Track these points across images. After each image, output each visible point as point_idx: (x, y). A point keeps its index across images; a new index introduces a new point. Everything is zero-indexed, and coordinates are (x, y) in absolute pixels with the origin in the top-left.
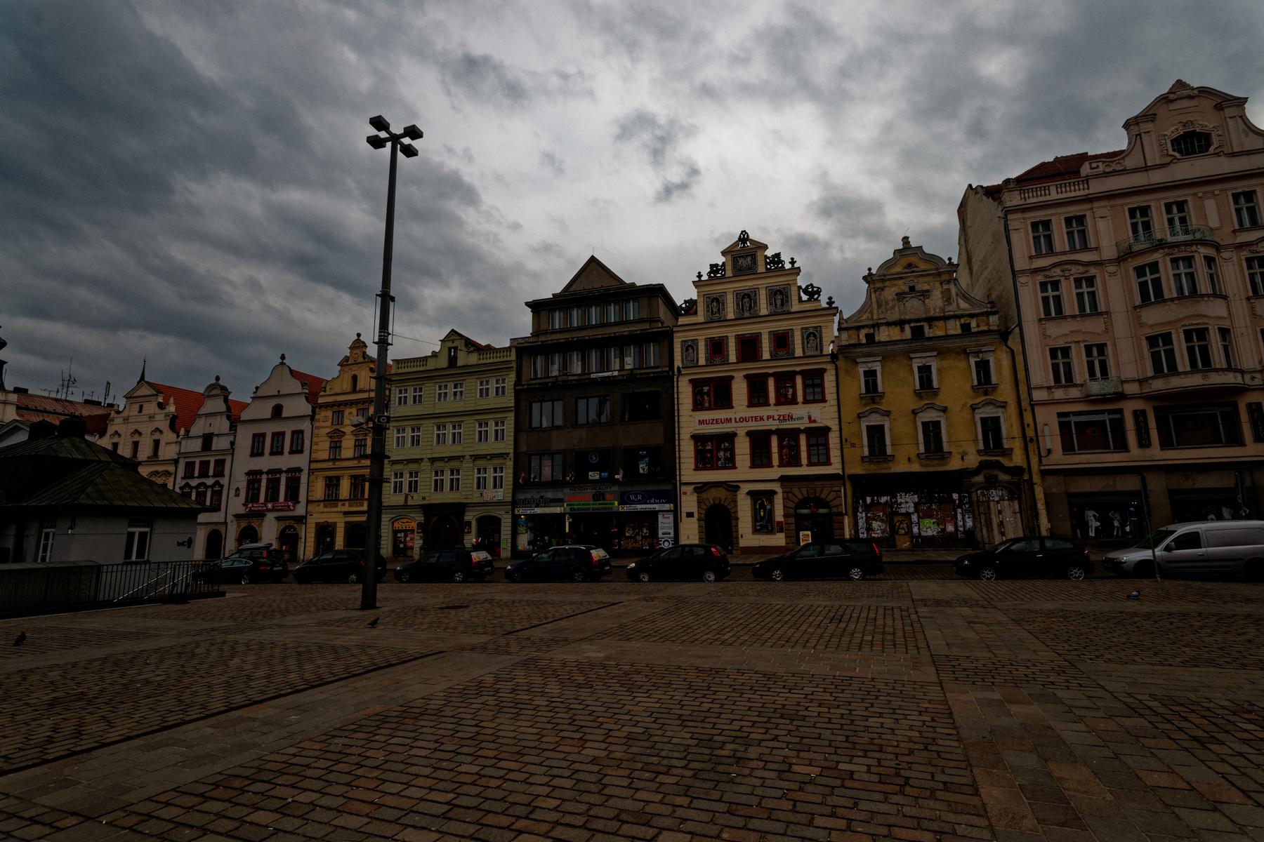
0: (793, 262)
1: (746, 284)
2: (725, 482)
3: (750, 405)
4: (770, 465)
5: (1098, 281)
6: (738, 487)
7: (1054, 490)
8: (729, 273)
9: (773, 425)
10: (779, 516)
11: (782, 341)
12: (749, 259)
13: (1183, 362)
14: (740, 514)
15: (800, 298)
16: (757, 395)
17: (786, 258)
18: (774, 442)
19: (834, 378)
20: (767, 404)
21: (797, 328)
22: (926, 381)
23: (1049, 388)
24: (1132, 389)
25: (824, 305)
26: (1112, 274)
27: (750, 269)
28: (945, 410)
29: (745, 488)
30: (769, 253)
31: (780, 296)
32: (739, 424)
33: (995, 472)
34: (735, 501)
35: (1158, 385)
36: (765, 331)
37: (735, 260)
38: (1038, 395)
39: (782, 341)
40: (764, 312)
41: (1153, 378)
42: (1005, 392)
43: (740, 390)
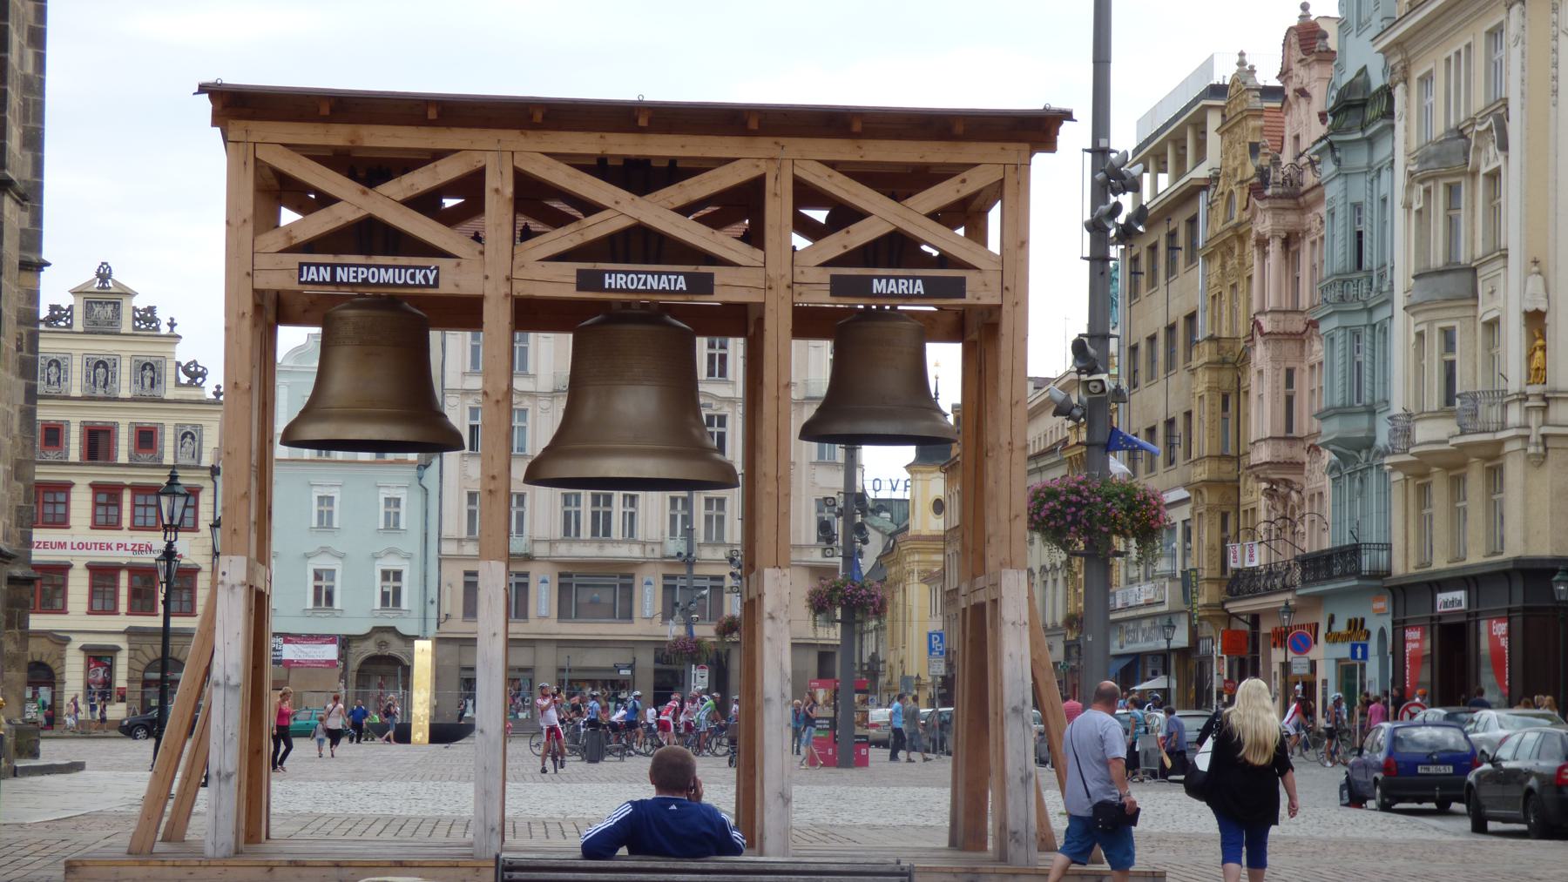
0: (172, 325)
1: (102, 347)
2: (50, 632)
3: (95, 526)
4: (114, 611)
5: (529, 415)
6: (68, 640)
7: (447, 662)
8: (78, 326)
9: (123, 557)
10: (121, 680)
11: (146, 438)
12: (110, 308)
13: (586, 532)
14: (67, 676)
15: (178, 379)
16: (105, 518)
17: (163, 316)
18: (124, 578)
19: (211, 500)
20: (117, 526)
21: (169, 424)
22: (325, 521)
23: (460, 540)
24: (541, 550)
25: (210, 395)
26: (545, 410)
27: (110, 323)
28: (341, 557)
29: (78, 642)
30: (140, 302)
31: (149, 370)
32: (77, 552)
33: (387, 637)
34: (62, 658)
35: (565, 551)
36: (124, 423)
37: (89, 306)
38: (449, 548)
39: (146, 438)
40: (125, 393)
41: (561, 541)
42: (413, 544)
43: (81, 504)
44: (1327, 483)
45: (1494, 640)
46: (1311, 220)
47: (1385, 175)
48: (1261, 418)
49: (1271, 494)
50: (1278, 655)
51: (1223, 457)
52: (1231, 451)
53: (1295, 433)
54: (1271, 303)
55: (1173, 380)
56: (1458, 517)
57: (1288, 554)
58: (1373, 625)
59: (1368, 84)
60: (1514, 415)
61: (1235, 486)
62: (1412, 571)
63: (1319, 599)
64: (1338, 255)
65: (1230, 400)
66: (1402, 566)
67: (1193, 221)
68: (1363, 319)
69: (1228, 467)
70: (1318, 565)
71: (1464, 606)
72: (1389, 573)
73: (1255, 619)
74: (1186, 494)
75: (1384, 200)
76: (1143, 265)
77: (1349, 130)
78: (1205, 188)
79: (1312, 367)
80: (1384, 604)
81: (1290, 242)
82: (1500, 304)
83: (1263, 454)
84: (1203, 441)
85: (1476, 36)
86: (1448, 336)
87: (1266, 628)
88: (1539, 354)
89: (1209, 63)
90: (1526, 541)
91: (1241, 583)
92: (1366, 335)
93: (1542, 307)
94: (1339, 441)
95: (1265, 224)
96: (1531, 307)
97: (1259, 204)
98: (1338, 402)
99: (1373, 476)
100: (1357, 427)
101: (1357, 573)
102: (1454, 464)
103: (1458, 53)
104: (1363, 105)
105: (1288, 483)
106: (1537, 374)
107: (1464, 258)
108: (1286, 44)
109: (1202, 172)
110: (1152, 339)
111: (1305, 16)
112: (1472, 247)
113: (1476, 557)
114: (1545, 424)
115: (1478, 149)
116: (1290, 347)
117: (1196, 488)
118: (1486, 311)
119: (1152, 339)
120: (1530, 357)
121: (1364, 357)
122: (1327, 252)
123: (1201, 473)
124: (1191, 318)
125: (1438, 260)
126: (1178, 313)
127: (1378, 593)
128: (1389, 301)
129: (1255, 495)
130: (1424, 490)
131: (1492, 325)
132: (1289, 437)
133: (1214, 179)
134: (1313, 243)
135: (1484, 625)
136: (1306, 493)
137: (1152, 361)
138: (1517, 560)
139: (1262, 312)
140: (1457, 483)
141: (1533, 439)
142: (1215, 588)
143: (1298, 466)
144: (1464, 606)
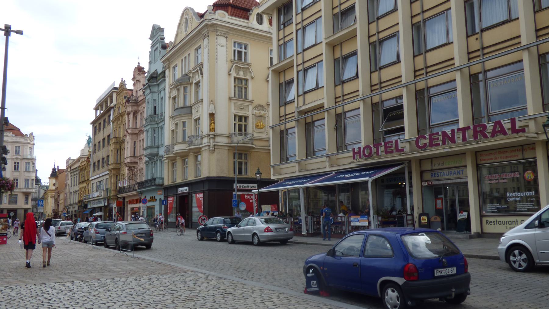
44: (144, 166)
45: (198, 199)
46: (141, 108)
47: (162, 92)
48: (128, 152)
49: (129, 170)
50: (130, 206)
51: (117, 163)
52: (119, 162)
53: (136, 155)
54: (131, 126)
55: (104, 150)
56: (184, 169)
57: (133, 182)
58: (158, 198)
59: (157, 73)
60: (205, 140)
61: (119, 170)
62: (170, 183)
63: (142, 193)
64: (151, 112)
65: (119, 150)
66: (167, 182)
67: (109, 116)
68: (156, 126)
69: (118, 165)
70: (141, 185)
71: (187, 191)
72: (163, 185)
73: (124, 198)
74: (107, 172)
75: (162, 98)
76: (98, 127)
77: (153, 82)
78: (113, 108)
79: (140, 141)
80: (161, 192)
81: (135, 113)
82: (200, 113)
83: (128, 160)
84: (112, 160)
85: (192, 52)
86: (184, 123)
87: (127, 200)
88: (213, 124)
89: (114, 83)
90: (209, 173)
91: (122, 190)
92: (157, 129)
93: (214, 112)
94: (150, 154)
95: (129, 109)
96: (211, 112)
97: (128, 105)
98: (149, 145)
99: (158, 162)
100: (154, 151)
101: (156, 185)
102: (184, 156)
103: (185, 57)
104: (156, 77)
105: (134, 167)
106: (212, 129)
107: (188, 104)
108: (135, 71)
109: (112, 105)
110: (99, 142)
111: (139, 65)
112: (191, 100)
113: (191, 177)
114: (214, 142)
115: (193, 77)
116: (135, 136)
117: (110, 170)
118: (195, 116)
119: (99, 142)
120: (210, 125)
121: (156, 135)
122: (146, 110)
123: (111, 167)
124: (109, 136)
125: (181, 105)
126: (106, 136)
127: (159, 190)
128: (164, 120)
129: (125, 171)
130: (173, 165)
131: (197, 120)
132: (134, 156)
133: (115, 105)
134: (141, 113)
135: (194, 195)
136: (138, 169)
137: (99, 147)
138: (207, 177)
139: (128, 129)
140: (184, 162)
141: (211, 146)
142: (114, 192)
143: (136, 163)
144: (187, 191)
